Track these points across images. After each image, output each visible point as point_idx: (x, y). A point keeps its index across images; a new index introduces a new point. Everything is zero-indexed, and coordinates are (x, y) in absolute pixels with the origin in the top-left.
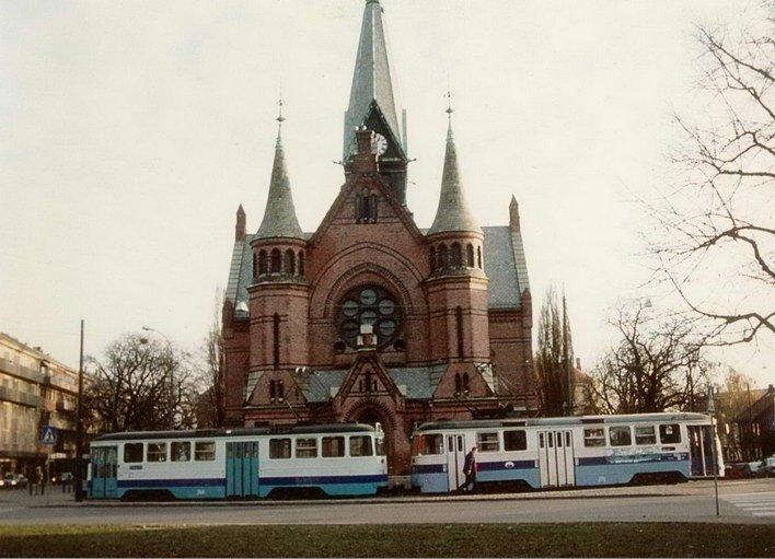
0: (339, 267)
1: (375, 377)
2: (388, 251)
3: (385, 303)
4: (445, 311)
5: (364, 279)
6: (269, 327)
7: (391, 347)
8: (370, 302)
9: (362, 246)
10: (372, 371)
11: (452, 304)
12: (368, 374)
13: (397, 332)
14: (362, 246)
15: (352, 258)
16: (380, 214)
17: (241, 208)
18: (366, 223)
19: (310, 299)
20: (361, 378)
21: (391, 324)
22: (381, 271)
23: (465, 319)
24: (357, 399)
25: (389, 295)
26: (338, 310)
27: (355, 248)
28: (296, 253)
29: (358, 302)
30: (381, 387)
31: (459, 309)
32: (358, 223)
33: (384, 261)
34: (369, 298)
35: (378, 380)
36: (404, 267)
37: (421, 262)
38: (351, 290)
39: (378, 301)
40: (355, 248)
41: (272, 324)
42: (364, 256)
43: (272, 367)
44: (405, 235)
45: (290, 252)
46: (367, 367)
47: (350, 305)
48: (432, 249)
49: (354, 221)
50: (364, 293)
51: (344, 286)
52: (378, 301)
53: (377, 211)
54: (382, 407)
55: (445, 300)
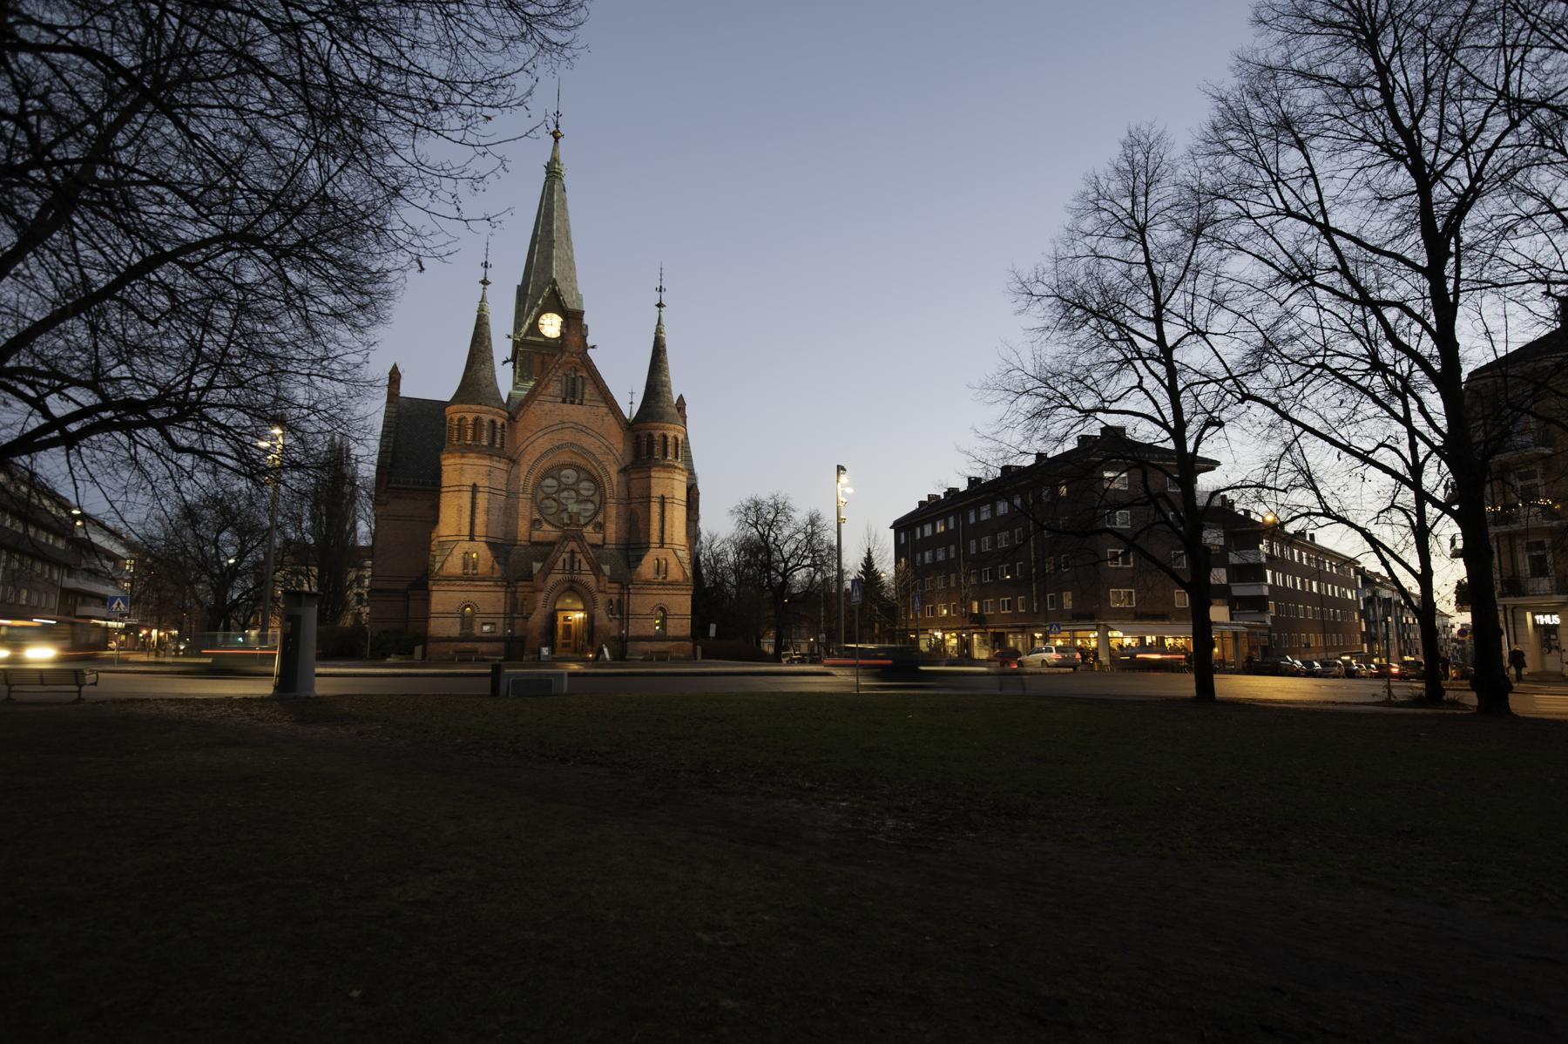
0: (543, 444)
1: (579, 556)
3: (585, 484)
5: (565, 457)
6: (466, 498)
8: (570, 481)
11: (656, 491)
12: (573, 552)
13: (596, 513)
16: (587, 396)
17: (395, 369)
18: (572, 403)
19: (509, 473)
20: (565, 556)
21: (590, 506)
22: (584, 452)
23: (668, 506)
25: (592, 479)
26: (538, 486)
28: (499, 425)
29: (558, 480)
30: (585, 566)
31: (663, 497)
32: (564, 401)
33: (587, 442)
34: (569, 475)
37: (618, 443)
38: (552, 468)
39: (579, 481)
42: (568, 436)
44: (610, 419)
45: (493, 422)
46: (573, 545)
47: (549, 482)
48: (638, 437)
50: (565, 472)
51: (546, 464)
52: (579, 481)
54: (585, 586)
55: (649, 488)
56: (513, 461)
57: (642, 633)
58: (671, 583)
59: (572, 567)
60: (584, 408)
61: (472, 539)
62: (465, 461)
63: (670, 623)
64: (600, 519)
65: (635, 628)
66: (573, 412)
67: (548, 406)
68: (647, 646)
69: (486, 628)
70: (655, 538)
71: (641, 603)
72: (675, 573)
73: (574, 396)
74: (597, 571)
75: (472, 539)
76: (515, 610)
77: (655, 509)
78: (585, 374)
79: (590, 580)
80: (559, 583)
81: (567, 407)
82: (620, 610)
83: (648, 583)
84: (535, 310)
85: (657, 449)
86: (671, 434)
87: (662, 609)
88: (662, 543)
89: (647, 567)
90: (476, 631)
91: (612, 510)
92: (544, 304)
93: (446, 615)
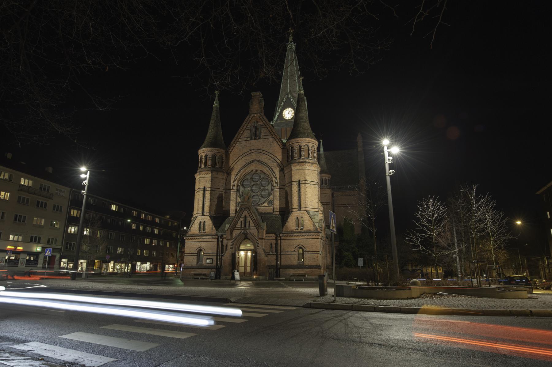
0: (241, 163)
1: (249, 219)
2: (266, 153)
4: (291, 182)
7: (266, 204)
9: (253, 151)
11: (295, 178)
12: (245, 217)
14: (253, 151)
16: (262, 134)
18: (255, 139)
20: (242, 219)
23: (302, 186)
24: (239, 231)
30: (252, 224)
31: (299, 181)
32: (251, 139)
35: (251, 221)
42: (254, 157)
43: (201, 214)
46: (245, 213)
49: (249, 139)
51: (243, 172)
53: (260, 133)
54: (252, 235)
57: (289, 263)
58: (306, 232)
59: (245, 226)
60: (261, 141)
61: (203, 215)
62: (201, 176)
63: (306, 256)
64: (271, 198)
66: (256, 144)
67: (244, 143)
68: (291, 272)
69: (208, 261)
70: (295, 205)
71: (290, 245)
72: (308, 225)
73: (256, 136)
74: (258, 226)
75: (203, 215)
76: (221, 250)
77: (295, 188)
78: (261, 123)
79: (255, 232)
80: (239, 235)
81: (253, 142)
82: (277, 250)
83: (292, 232)
84: (280, 108)
85: (296, 154)
88: (300, 207)
89: (291, 223)
91: (277, 193)
92: (284, 104)
93: (191, 254)
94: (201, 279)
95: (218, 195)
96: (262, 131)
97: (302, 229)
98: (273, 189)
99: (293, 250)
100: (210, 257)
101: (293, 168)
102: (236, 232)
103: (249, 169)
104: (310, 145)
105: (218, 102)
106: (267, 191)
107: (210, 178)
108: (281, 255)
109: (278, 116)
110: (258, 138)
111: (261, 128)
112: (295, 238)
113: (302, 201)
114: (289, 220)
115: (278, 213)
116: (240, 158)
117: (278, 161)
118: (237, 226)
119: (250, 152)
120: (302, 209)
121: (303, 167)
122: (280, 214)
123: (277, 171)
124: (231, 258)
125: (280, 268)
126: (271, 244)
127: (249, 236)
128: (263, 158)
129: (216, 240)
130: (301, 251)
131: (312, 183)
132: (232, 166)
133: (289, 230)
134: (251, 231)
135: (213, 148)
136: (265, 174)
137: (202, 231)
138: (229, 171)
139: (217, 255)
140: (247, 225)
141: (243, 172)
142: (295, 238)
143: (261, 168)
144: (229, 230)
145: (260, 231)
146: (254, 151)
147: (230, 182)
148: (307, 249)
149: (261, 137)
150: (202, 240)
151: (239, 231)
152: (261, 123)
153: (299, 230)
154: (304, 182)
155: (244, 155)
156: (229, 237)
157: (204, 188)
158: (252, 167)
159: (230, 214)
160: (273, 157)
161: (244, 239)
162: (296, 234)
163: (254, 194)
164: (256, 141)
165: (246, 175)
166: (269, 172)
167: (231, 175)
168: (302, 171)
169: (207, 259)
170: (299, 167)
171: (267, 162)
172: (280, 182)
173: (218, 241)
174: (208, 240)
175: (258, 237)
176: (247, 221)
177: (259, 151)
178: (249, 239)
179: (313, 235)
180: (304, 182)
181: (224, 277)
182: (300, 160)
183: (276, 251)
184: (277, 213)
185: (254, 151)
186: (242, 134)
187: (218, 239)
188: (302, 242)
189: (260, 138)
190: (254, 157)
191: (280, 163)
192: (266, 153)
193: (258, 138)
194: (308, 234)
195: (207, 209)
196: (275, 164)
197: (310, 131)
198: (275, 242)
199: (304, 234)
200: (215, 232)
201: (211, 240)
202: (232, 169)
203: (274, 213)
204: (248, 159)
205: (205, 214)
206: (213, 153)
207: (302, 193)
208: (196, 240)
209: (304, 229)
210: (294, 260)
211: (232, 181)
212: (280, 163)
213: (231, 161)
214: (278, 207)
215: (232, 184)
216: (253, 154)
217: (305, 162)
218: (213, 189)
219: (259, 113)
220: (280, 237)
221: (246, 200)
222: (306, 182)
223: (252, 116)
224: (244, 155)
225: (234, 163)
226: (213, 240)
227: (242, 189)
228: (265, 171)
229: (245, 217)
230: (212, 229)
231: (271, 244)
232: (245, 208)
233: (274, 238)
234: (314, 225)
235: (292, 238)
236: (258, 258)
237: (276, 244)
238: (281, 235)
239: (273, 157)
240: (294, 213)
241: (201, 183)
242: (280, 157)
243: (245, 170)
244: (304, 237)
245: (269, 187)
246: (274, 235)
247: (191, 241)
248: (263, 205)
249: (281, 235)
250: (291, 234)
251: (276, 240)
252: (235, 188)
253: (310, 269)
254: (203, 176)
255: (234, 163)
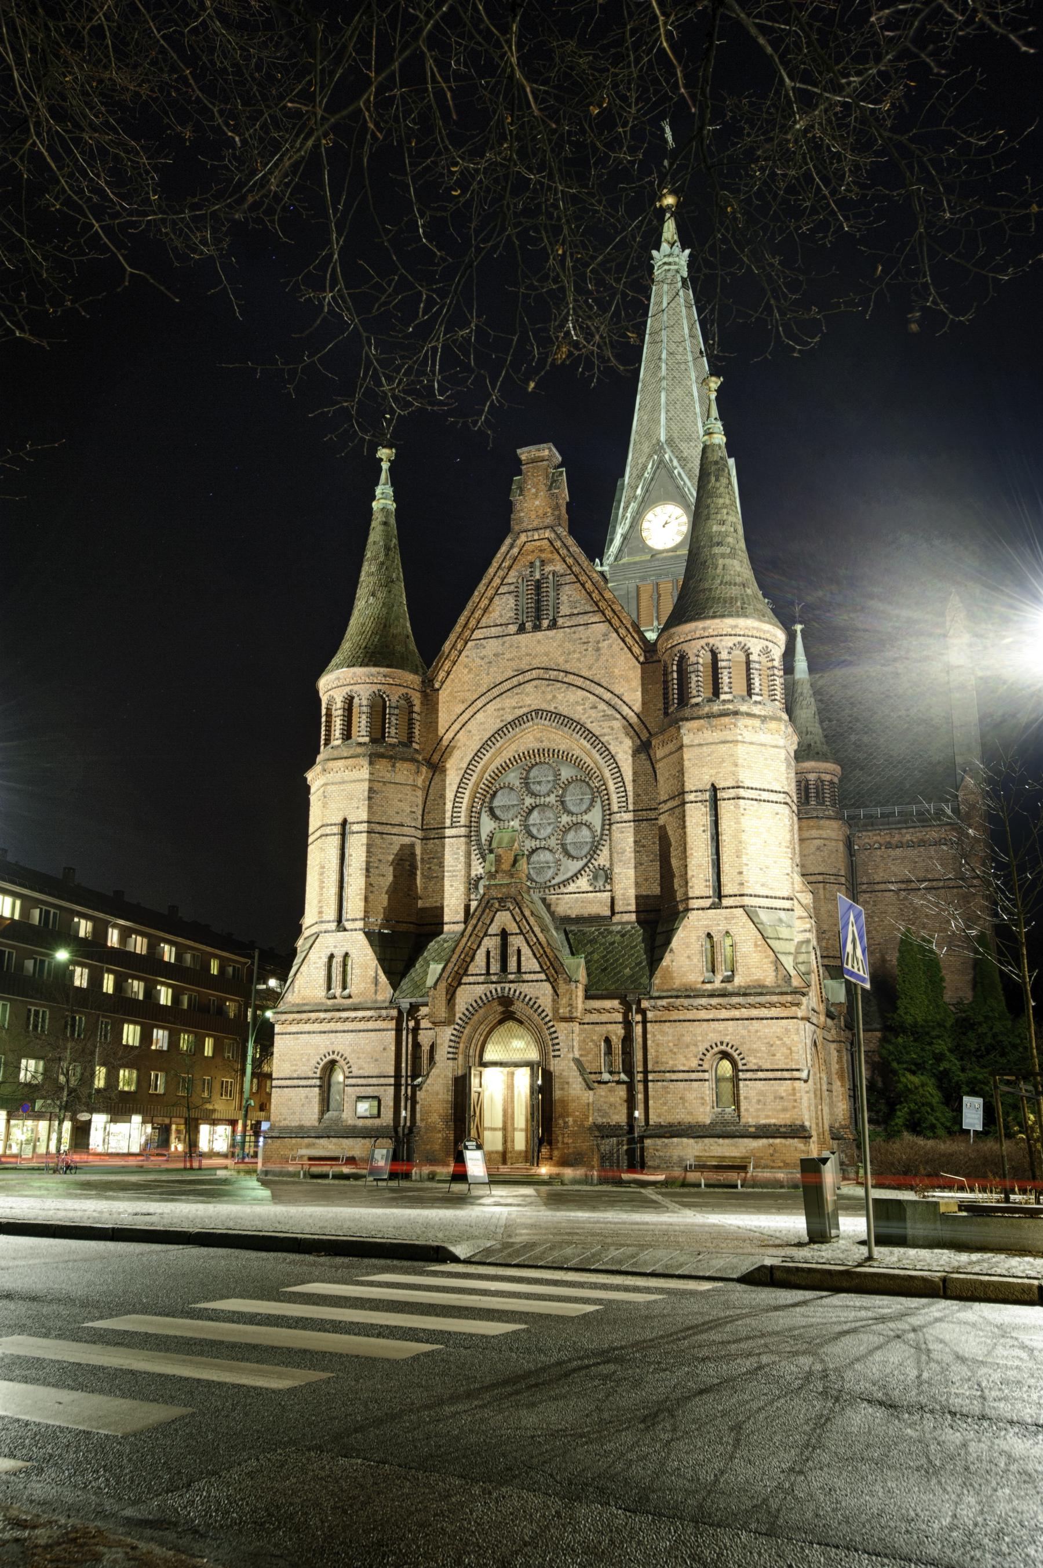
0: (487, 721)
1: (516, 942)
2: (579, 682)
4: (680, 794)
7: (583, 883)
9: (528, 676)
10: (513, 928)
11: (697, 778)
12: (504, 935)
14: (528, 676)
15: (509, 702)
16: (564, 610)
18: (537, 628)
20: (491, 943)
24: (480, 990)
27: (515, 681)
30: (530, 963)
31: (714, 789)
32: (522, 629)
35: (526, 951)
36: (611, 712)
40: (515, 681)
41: (336, 841)
42: (532, 698)
43: (333, 926)
46: (503, 919)
49: (513, 628)
51: (493, 760)
53: (556, 608)
54: (532, 1004)
56: (436, 767)
57: (680, 1116)
59: (504, 968)
65: (665, 1105)
67: (492, 646)
68: (690, 1149)
69: (363, 1108)
71: (679, 1042)
73: (538, 618)
74: (553, 971)
76: (411, 1064)
77: (697, 817)
78: (559, 567)
79: (542, 992)
82: (629, 1064)
83: (690, 993)
84: (633, 506)
86: (724, 645)
87: (725, 1055)
89: (684, 957)
90: (348, 1117)
91: (625, 837)
93: (296, 1082)
94: (336, 1177)
95: (395, 849)
96: (564, 598)
97: (729, 980)
98: (608, 823)
99: (694, 1063)
100: (370, 1091)
101: (686, 740)
102: (466, 996)
103: (513, 747)
104: (755, 647)
105: (389, 491)
106: (585, 831)
107: (366, 786)
108: (646, 1081)
109: (625, 537)
110: (545, 623)
111: (558, 586)
112: (703, 1014)
113: (725, 868)
114: (675, 943)
115: (633, 917)
116: (479, 704)
117: (626, 710)
118: (472, 969)
119: (521, 678)
120: (726, 902)
121: (727, 735)
122: (638, 921)
123: (623, 750)
124: (450, 1097)
125: (642, 1138)
126: (607, 1041)
127: (518, 1007)
128: (570, 701)
129: (392, 1025)
130: (726, 1066)
131: (765, 795)
132: (450, 735)
133: (677, 984)
134: (524, 988)
135: (373, 670)
136: (577, 763)
137: (337, 990)
138: (436, 757)
139: (397, 1086)
140: (512, 965)
141: (491, 761)
142: (703, 1014)
143: (561, 740)
144: (442, 985)
145: (562, 988)
146: (534, 674)
147: (443, 797)
148: (753, 1062)
149: (560, 621)
150: (340, 1026)
151: (480, 990)
152: (559, 567)
153: (717, 984)
154: (732, 793)
155: (496, 692)
156: (442, 1013)
157: (344, 823)
158: (528, 739)
159: (442, 924)
160: (607, 696)
161: (501, 1022)
162: (703, 1001)
163: (534, 844)
164: (539, 635)
165: (504, 768)
166: (593, 758)
167: (444, 771)
168: (723, 748)
169: (360, 1098)
170: (708, 736)
171: (583, 719)
172: (637, 795)
173: (399, 1031)
174: (362, 1025)
175: (556, 1010)
176: (511, 950)
177: (552, 675)
178: (521, 1023)
179: (773, 1005)
180: (732, 793)
181: (426, 1170)
182: (716, 708)
183: (629, 1070)
184: (626, 918)
185: (534, 674)
186: (485, 610)
187: (399, 1020)
188: (730, 1033)
189: (553, 625)
190: (532, 698)
191: (634, 719)
192: (579, 682)
193: (545, 623)
194: (751, 1000)
195: (354, 906)
196: (618, 724)
197: (753, 589)
198: (620, 1031)
199: (735, 1000)
200: (386, 991)
201: (371, 1025)
202: (447, 751)
203: (616, 918)
204: (511, 705)
205: (348, 925)
206: (375, 688)
207: (725, 838)
208: (316, 1027)
209: (738, 981)
210: (699, 1103)
211: (450, 795)
212: (634, 719)
213: (444, 718)
214: (632, 892)
215: (449, 806)
216: (529, 687)
217: (736, 713)
218: (376, 828)
219: (552, 528)
220: (643, 1012)
221: (506, 866)
222: (742, 792)
223: (523, 538)
224: (496, 692)
225: (457, 726)
226: (380, 1024)
227: (487, 825)
228: (577, 752)
229: (504, 935)
230: (376, 982)
231: (607, 1041)
232: (501, 900)
233: (619, 1017)
234: (777, 963)
235: (690, 1015)
236: (557, 1094)
237: (628, 1039)
238: (645, 1004)
239: (607, 696)
240: (692, 915)
241: (333, 805)
242: (635, 697)
243: (499, 751)
244: (736, 1013)
245: (595, 817)
246: (616, 1003)
247: (294, 1028)
248: (572, 887)
249: (645, 1004)
250: (686, 1002)
251: (628, 1025)
252: (463, 821)
253: (764, 1141)
254: (338, 777)
255: (457, 726)
